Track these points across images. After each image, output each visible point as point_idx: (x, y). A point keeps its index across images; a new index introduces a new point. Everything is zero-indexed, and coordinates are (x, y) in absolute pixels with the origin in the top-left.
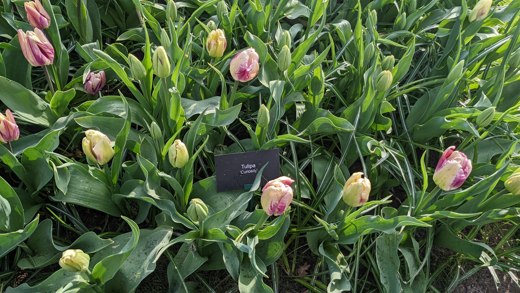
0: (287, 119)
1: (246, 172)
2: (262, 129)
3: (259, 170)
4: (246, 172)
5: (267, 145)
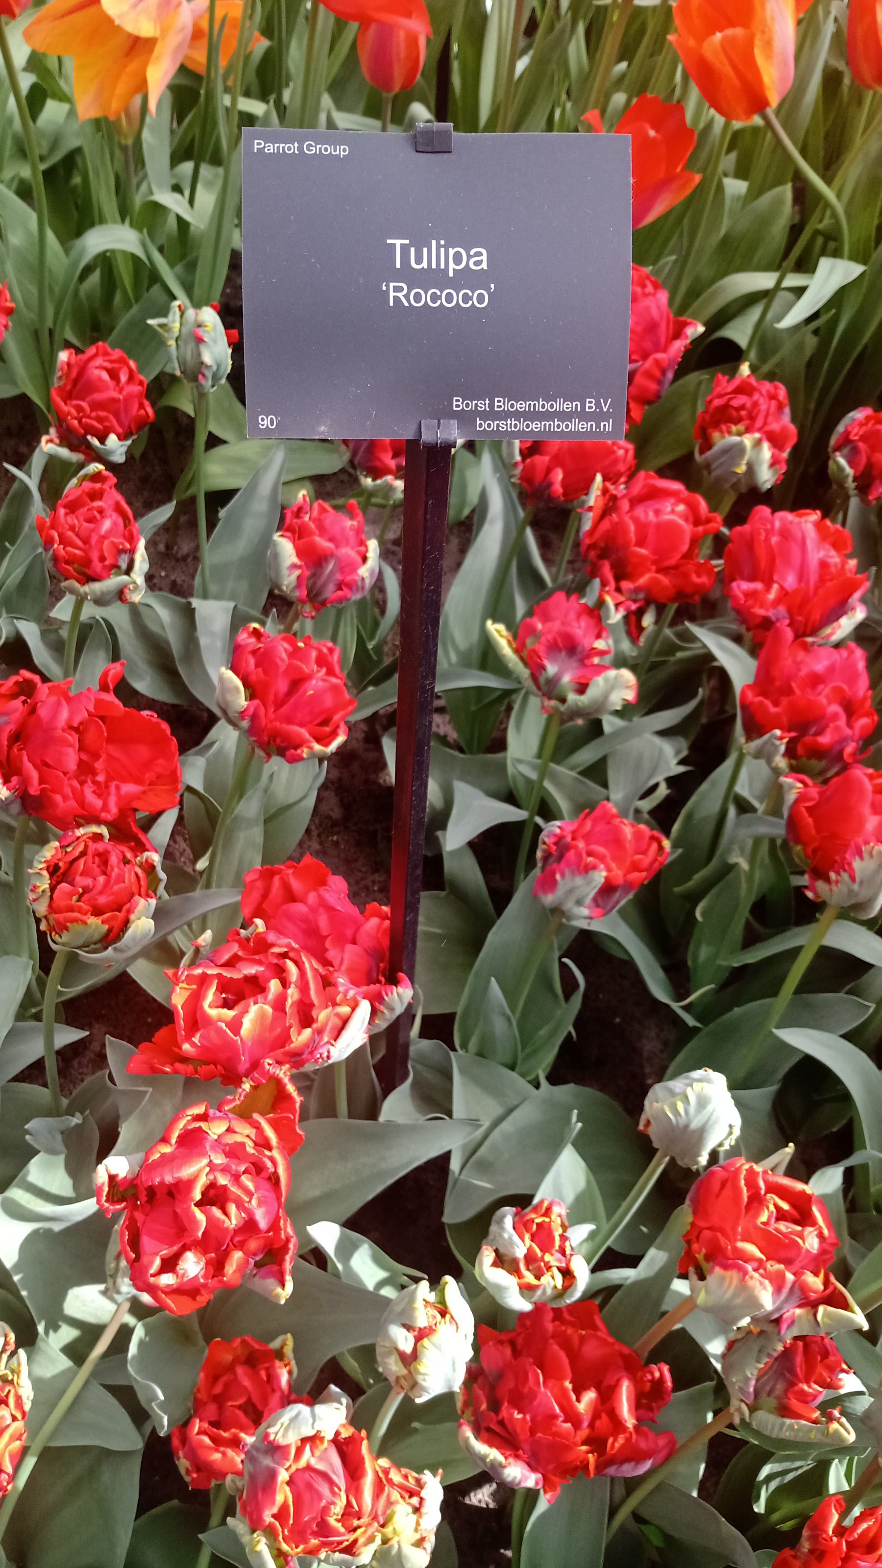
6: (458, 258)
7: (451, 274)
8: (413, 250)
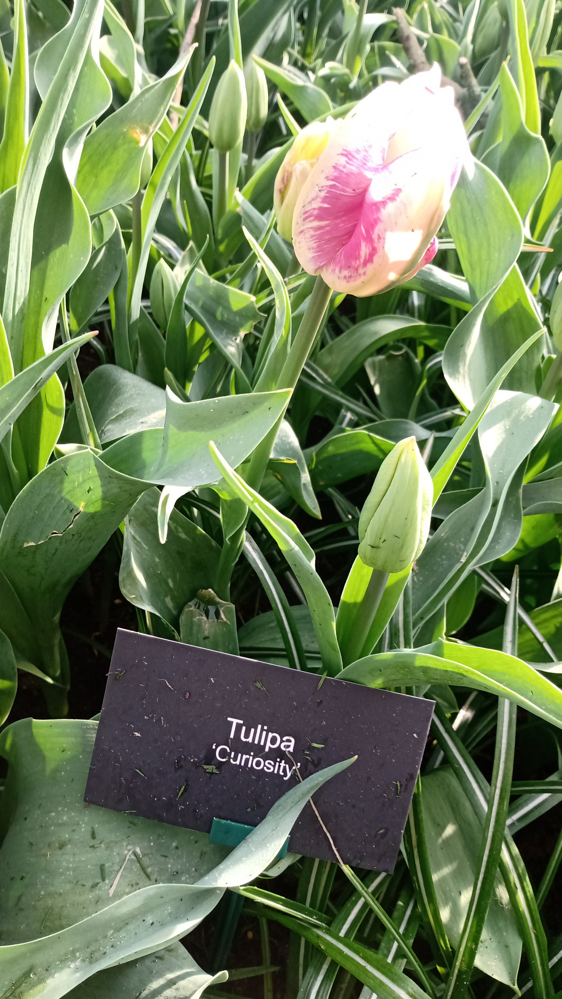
0: (515, 580)
1: (241, 760)
2: (378, 578)
3: (306, 773)
4: (241, 760)
5: (377, 667)
6: (273, 741)
7: (267, 749)
8: (244, 728)
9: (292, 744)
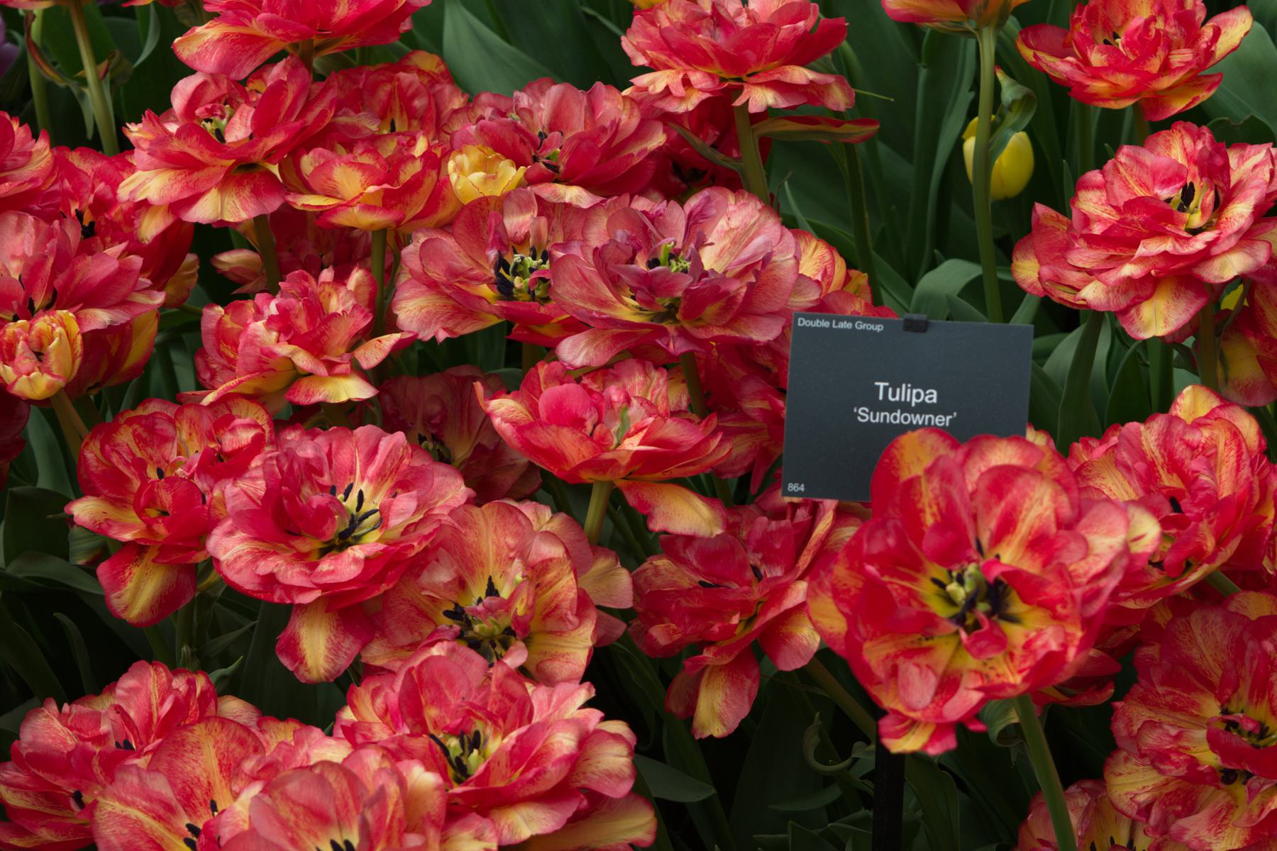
6: (918, 396)
8: (890, 390)
9: (935, 396)
